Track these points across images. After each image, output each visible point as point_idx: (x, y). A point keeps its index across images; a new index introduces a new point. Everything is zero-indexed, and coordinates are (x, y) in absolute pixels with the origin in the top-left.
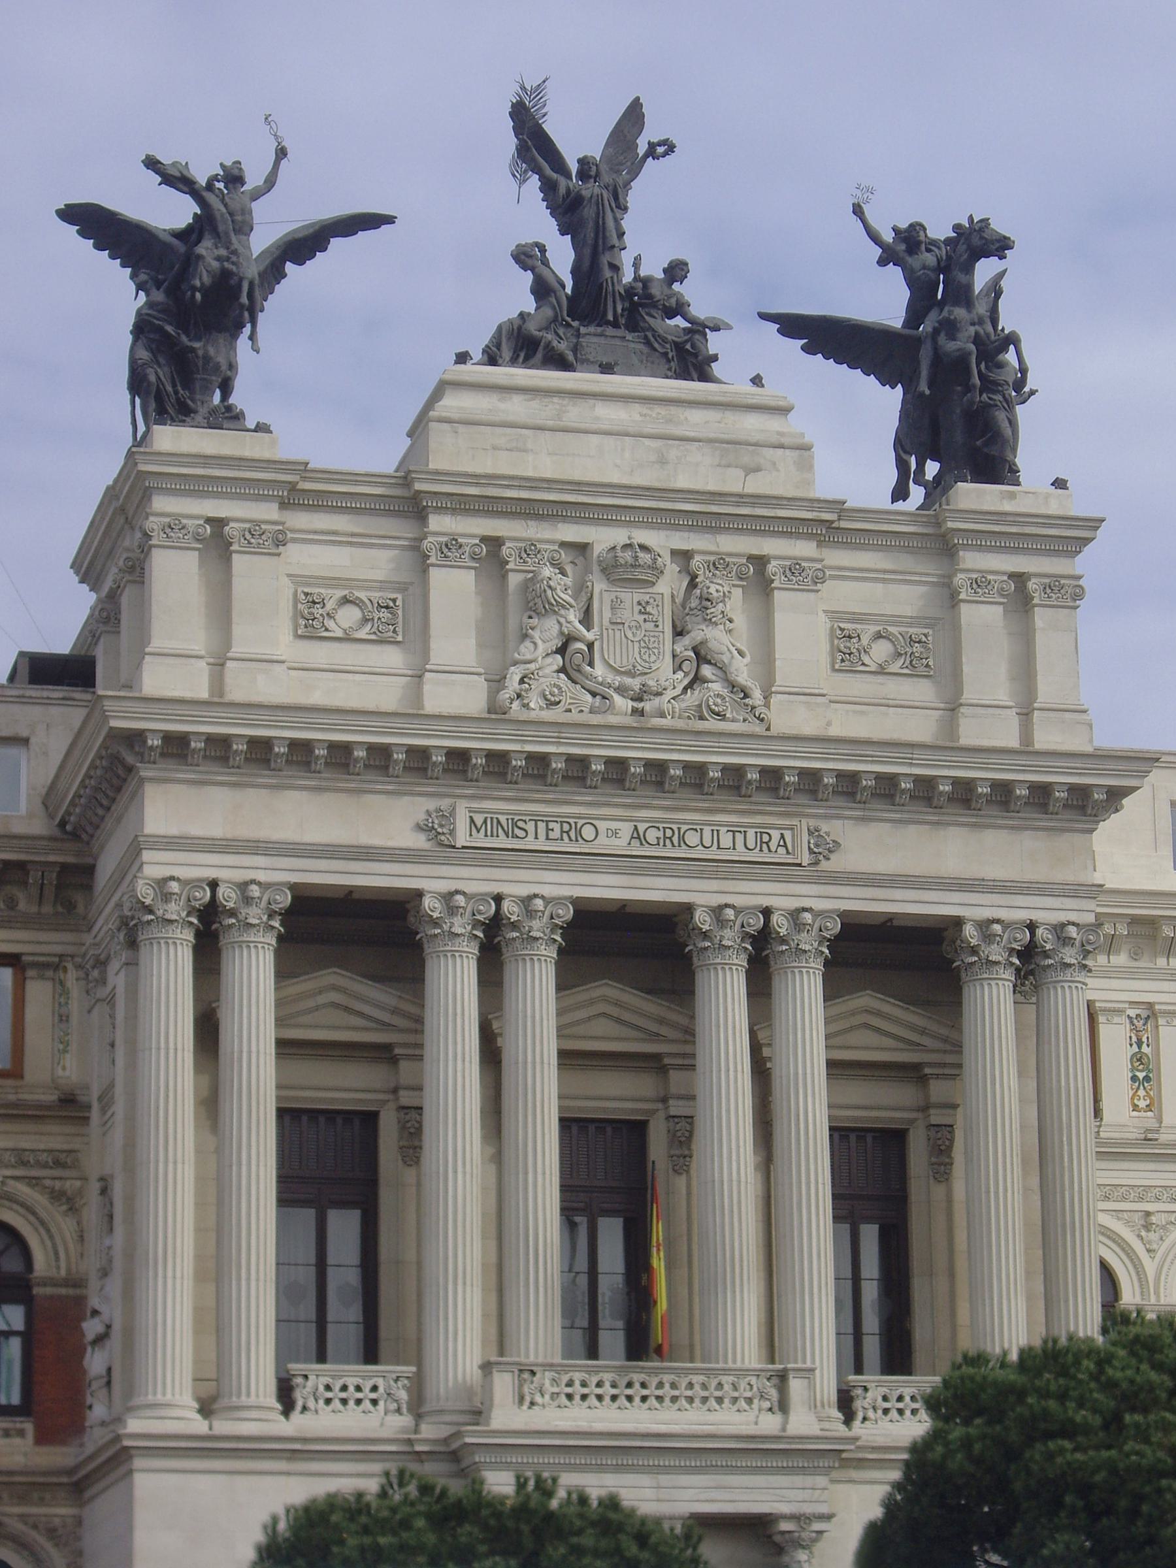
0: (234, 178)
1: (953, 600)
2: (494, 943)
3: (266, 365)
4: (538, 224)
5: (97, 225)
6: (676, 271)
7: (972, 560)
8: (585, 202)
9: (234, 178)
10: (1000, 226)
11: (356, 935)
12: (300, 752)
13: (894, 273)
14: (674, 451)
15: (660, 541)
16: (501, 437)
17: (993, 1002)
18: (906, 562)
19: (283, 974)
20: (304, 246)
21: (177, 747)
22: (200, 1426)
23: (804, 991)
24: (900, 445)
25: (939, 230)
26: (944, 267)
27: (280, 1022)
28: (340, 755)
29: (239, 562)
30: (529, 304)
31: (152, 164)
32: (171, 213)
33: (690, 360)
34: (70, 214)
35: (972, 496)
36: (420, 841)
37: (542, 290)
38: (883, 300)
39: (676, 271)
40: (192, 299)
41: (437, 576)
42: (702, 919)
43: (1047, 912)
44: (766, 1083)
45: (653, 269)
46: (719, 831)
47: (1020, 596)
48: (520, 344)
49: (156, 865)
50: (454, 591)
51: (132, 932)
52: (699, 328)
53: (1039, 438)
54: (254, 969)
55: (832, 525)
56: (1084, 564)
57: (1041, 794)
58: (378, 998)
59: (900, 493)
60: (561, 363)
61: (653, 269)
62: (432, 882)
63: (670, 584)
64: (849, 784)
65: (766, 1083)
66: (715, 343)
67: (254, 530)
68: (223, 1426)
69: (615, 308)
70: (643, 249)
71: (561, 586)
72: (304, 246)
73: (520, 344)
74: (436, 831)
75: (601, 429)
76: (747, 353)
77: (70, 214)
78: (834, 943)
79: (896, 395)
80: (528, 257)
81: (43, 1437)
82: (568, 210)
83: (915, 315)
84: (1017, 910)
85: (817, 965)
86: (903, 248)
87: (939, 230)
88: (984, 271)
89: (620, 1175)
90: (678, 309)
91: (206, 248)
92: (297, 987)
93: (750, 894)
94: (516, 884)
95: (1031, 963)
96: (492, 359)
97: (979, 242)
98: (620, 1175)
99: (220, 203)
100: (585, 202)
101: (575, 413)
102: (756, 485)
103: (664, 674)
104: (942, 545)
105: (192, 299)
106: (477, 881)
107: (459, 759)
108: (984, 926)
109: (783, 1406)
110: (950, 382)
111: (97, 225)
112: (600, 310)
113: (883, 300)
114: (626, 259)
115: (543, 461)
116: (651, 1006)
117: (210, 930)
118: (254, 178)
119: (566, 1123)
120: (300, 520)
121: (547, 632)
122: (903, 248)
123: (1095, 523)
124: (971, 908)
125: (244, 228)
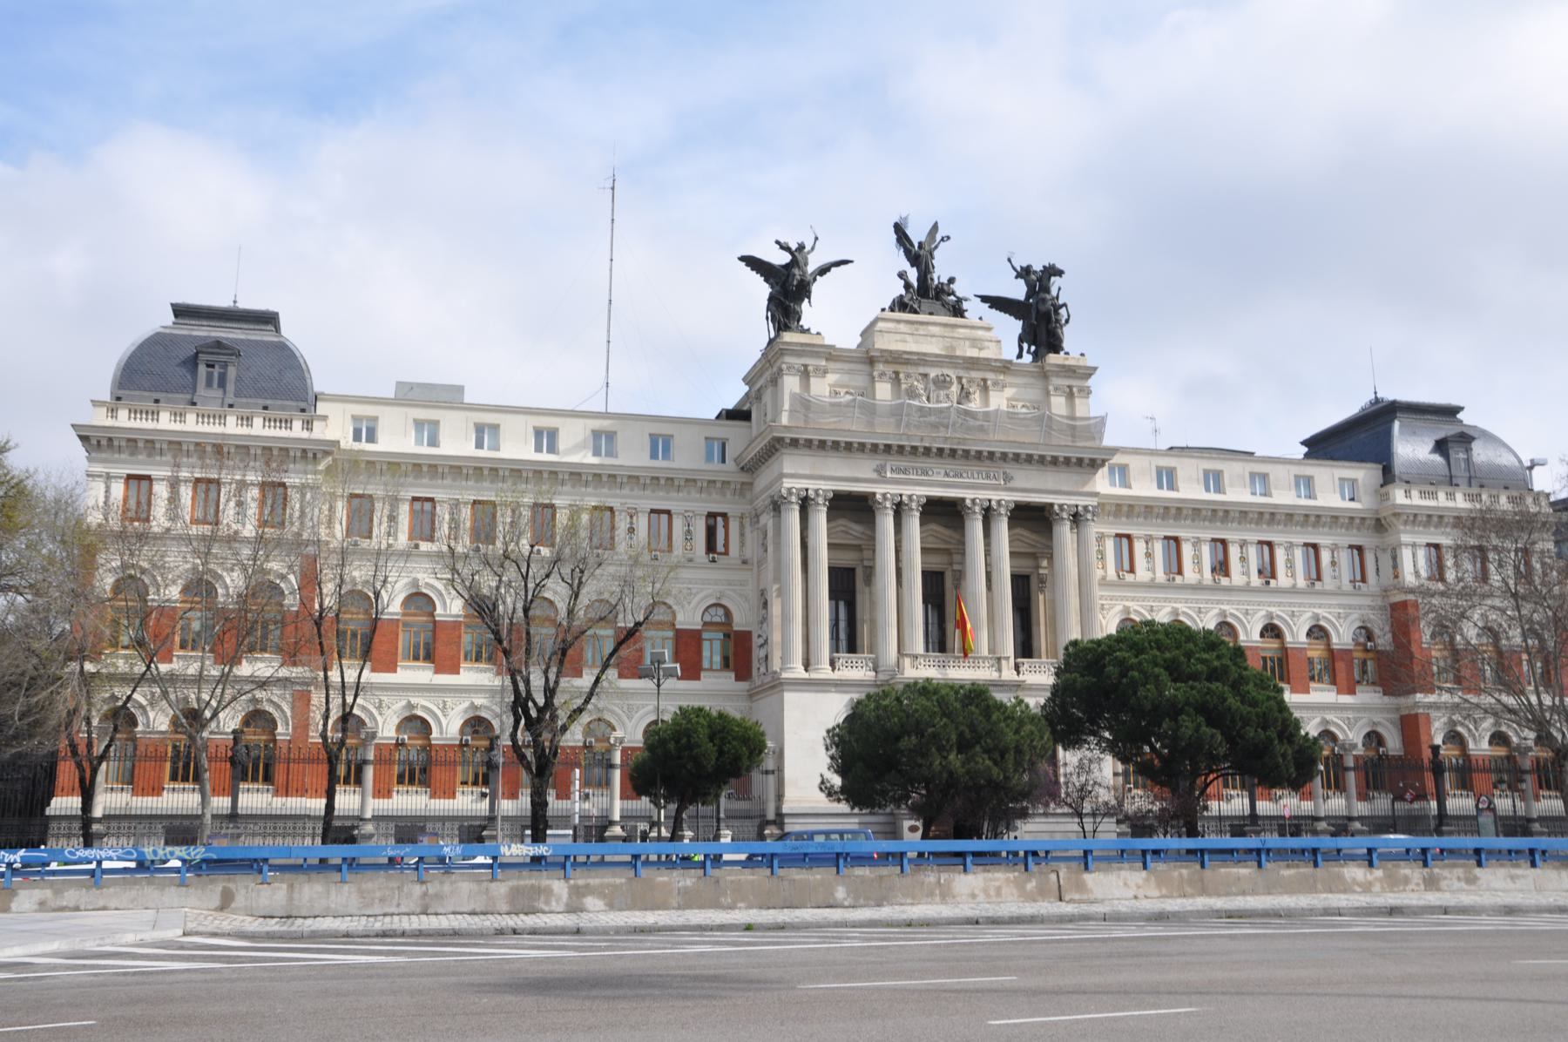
0: (801, 247)
1: (1048, 393)
2: (899, 509)
3: (812, 313)
4: (905, 265)
5: (753, 263)
6: (951, 280)
7: (1056, 381)
8: (919, 257)
9: (801, 247)
10: (1059, 266)
11: (853, 508)
12: (836, 445)
13: (1021, 282)
14: (955, 343)
15: (952, 374)
16: (898, 337)
17: (1065, 534)
18: (1032, 381)
19: (829, 520)
20: (823, 271)
21: (794, 443)
22: (806, 675)
23: (1002, 528)
24: (1021, 340)
25: (1037, 267)
26: (1039, 279)
27: (829, 536)
28: (849, 446)
29: (812, 380)
30: (903, 292)
31: (778, 242)
32: (781, 258)
33: (957, 310)
34: (742, 259)
35: (1052, 358)
36: (875, 476)
37: (908, 286)
38: (1017, 290)
39: (951, 280)
40: (788, 288)
41: (879, 386)
42: (968, 502)
43: (1082, 502)
44: (989, 558)
45: (944, 280)
47: (1070, 396)
49: (787, 483)
51: (777, 506)
52: (960, 300)
53: (1071, 337)
54: (820, 519)
55: (1005, 367)
56: (1090, 382)
57: (1080, 461)
58: (857, 529)
59: (1020, 356)
60: (916, 312)
61: (944, 280)
62: (879, 490)
63: (955, 388)
64: (1017, 457)
65: (989, 558)
66: (965, 305)
67: (817, 369)
68: (814, 675)
69: (932, 293)
70: (940, 274)
71: (920, 386)
72: (823, 271)
73: (900, 305)
74: (880, 470)
75: (926, 336)
76: (976, 310)
77: (742, 259)
78: (1012, 511)
79: (1020, 323)
80: (902, 275)
81: (738, 679)
83: (1028, 296)
84: (1072, 501)
85: (1005, 520)
86: (1024, 273)
87: (1037, 267)
88: (1055, 282)
89: (940, 592)
90: (953, 293)
91: (796, 271)
92: (833, 524)
93: (983, 495)
94: (907, 491)
95: (1077, 518)
96: (892, 310)
97: (1052, 271)
98: (940, 592)
99: (798, 255)
100: (919, 257)
101: (922, 330)
102: (983, 354)
104: (1044, 375)
105: (788, 288)
106: (893, 490)
107: (888, 448)
108: (1061, 506)
109: (999, 670)
110: (1039, 318)
111: (753, 263)
112: (926, 293)
113: (1018, 290)
114: (935, 277)
115: (911, 346)
116: (947, 532)
117: (805, 504)
118: (808, 248)
119: (924, 573)
120: (831, 365)
122: (1024, 273)
123: (1095, 369)
124: (1056, 500)
125: (806, 264)
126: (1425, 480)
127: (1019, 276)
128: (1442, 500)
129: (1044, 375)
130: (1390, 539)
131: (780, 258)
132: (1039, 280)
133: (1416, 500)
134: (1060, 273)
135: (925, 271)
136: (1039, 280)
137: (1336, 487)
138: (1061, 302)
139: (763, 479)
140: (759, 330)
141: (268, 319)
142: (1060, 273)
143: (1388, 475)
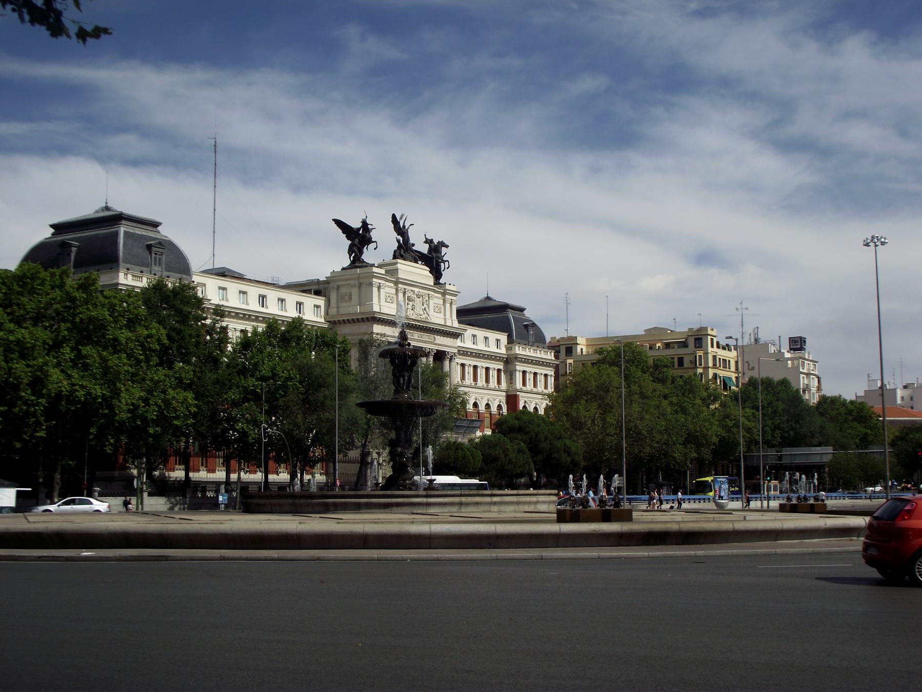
5: (339, 223)
8: (400, 230)
10: (447, 243)
25: (436, 242)
34: (334, 220)
46: (426, 337)
50: (401, 295)
77: (334, 220)
80: (398, 241)
86: (429, 241)
87: (436, 242)
88: (444, 250)
97: (442, 244)
100: (400, 230)
103: (421, 312)
111: (339, 223)
112: (405, 250)
121: (411, 303)
122: (429, 241)
127: (426, 242)
130: (511, 367)
131: (356, 224)
134: (447, 247)
138: (445, 259)
141: (155, 225)
142: (447, 247)
143: (510, 341)
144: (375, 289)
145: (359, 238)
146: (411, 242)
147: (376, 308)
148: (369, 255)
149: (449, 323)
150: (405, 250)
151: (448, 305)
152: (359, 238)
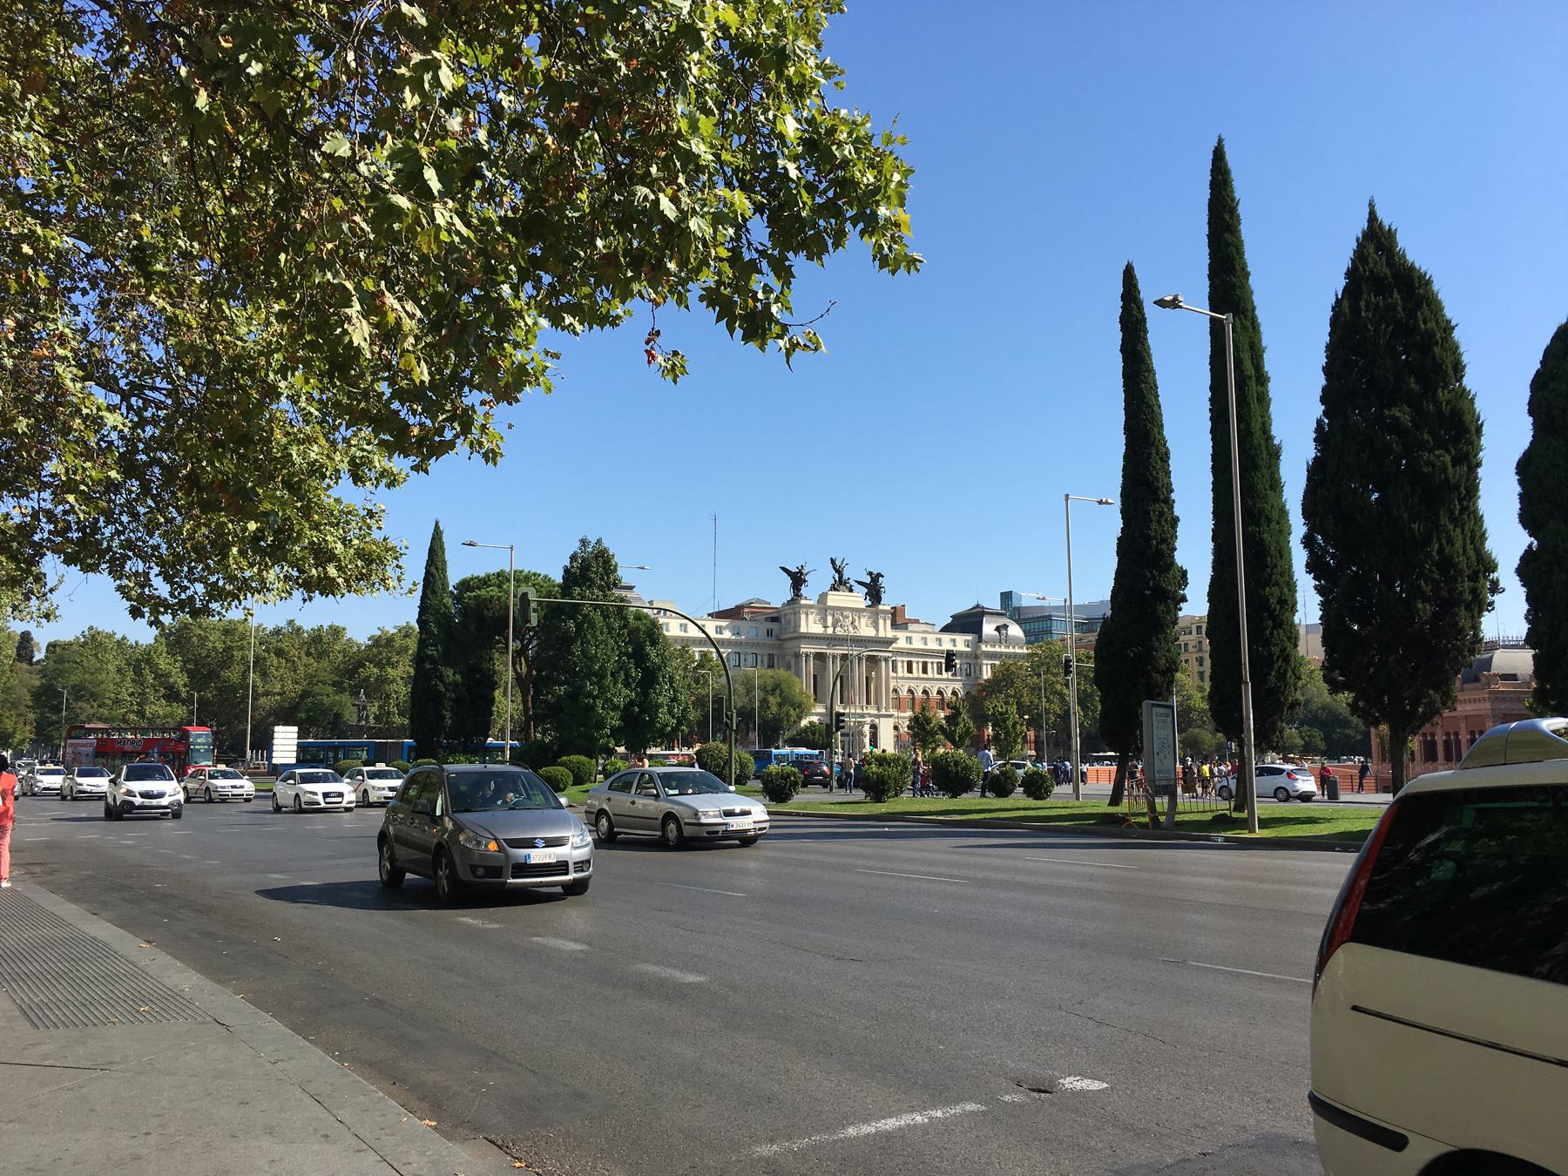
8: (839, 571)
11: (820, 657)
38: (868, 580)
48: (834, 588)
82: (837, 571)
86: (870, 574)
97: (880, 575)
100: (839, 571)
110: (874, 591)
113: (868, 580)
122: (870, 574)
126: (992, 642)
128: (997, 649)
129: (877, 613)
132: (876, 578)
133: (989, 649)
135: (841, 577)
136: (876, 578)
137: (960, 642)
139: (789, 644)
140: (789, 595)
144: (803, 617)
145: (797, 580)
146: (845, 577)
147: (803, 629)
148: (804, 590)
149: (882, 634)
150: (840, 583)
151: (881, 622)
152: (797, 580)
